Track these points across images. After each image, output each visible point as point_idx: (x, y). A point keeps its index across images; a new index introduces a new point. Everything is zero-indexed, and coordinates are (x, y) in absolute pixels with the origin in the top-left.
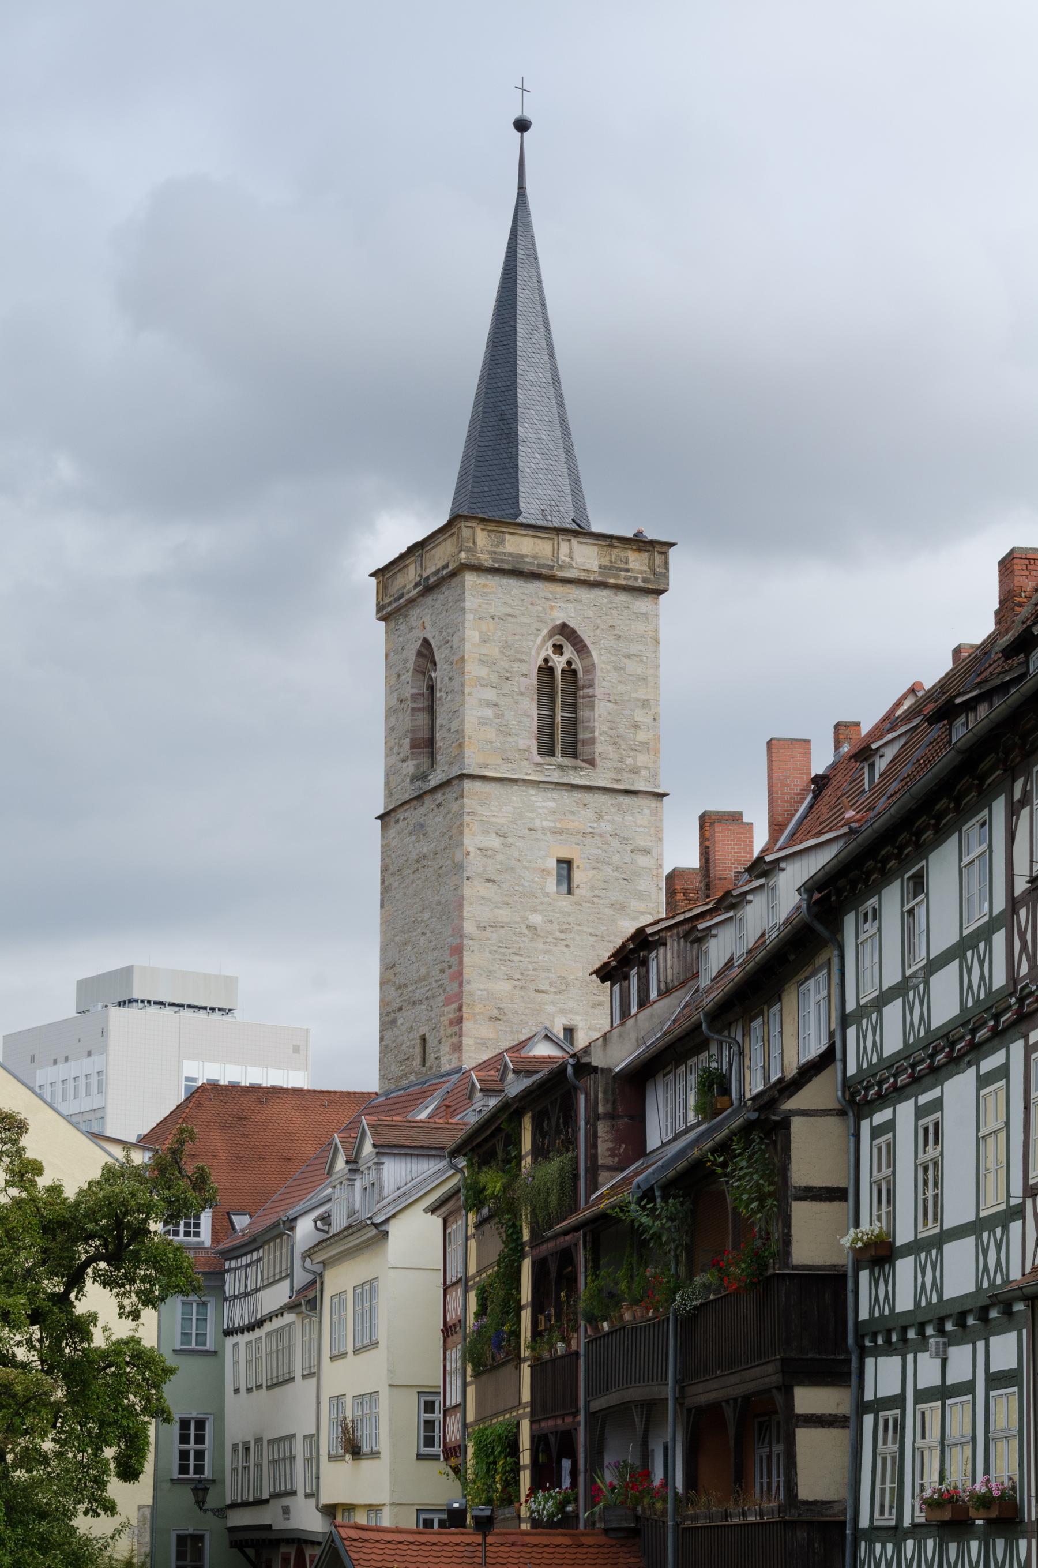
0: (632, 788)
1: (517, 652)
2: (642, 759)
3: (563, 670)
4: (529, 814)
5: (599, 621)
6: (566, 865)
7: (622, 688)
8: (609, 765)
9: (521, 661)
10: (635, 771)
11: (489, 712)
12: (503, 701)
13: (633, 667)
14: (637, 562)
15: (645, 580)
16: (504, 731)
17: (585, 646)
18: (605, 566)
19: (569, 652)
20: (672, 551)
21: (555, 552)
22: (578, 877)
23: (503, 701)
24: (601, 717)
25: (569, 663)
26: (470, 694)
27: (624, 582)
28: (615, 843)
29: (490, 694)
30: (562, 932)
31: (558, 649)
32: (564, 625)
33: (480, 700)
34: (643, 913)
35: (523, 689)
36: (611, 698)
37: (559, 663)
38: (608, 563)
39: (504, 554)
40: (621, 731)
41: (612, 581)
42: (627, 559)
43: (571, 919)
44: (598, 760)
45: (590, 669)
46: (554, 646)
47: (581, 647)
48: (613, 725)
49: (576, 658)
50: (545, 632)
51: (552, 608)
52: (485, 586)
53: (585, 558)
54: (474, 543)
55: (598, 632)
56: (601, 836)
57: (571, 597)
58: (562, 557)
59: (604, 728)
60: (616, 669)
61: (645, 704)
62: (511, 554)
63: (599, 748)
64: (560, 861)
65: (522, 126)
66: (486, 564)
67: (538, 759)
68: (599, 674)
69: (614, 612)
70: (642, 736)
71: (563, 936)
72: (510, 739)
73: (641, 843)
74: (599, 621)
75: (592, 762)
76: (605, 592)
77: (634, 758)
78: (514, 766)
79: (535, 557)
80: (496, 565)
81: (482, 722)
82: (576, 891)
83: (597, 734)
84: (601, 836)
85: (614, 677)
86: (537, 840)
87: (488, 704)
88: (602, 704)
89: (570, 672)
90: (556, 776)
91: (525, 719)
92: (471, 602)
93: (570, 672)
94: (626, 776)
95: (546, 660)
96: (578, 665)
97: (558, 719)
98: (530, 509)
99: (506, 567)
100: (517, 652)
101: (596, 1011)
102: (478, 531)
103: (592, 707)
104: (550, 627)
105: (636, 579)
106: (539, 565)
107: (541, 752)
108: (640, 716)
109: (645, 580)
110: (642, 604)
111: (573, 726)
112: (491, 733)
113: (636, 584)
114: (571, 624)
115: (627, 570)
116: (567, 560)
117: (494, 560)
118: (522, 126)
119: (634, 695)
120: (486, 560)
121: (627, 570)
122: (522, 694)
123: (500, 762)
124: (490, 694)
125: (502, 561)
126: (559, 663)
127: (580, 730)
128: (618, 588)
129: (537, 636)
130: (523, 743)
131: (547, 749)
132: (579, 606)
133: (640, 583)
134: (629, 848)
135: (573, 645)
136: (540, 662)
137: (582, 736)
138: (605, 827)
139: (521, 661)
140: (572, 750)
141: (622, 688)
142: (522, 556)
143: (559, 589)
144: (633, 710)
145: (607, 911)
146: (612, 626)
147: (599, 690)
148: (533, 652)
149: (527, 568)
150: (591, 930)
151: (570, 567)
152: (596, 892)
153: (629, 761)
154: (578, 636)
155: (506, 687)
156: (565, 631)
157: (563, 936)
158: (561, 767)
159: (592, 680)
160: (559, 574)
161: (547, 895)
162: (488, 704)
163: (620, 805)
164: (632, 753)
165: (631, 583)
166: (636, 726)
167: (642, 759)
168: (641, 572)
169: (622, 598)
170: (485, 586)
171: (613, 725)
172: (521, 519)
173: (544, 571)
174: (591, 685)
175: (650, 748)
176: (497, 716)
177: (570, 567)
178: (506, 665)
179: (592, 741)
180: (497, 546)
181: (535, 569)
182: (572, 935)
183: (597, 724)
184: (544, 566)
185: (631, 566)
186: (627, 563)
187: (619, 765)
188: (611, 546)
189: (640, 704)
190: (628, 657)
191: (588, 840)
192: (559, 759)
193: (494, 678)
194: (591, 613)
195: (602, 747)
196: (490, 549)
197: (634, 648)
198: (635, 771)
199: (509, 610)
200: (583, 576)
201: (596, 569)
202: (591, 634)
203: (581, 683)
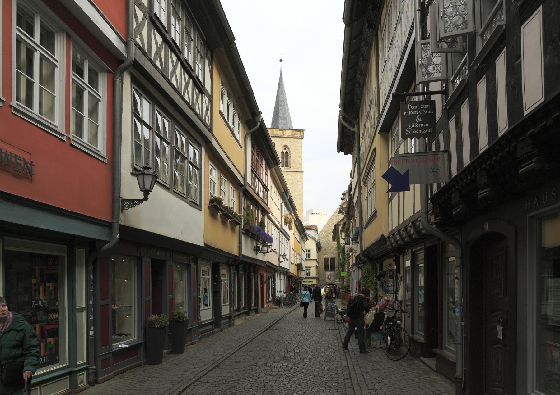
2: (299, 166)
10: (298, 168)
13: (297, 151)
14: (298, 134)
20: (304, 132)
24: (292, 160)
31: (285, 149)
37: (285, 151)
45: (290, 152)
53: (288, 133)
61: (300, 157)
65: (281, 61)
70: (299, 162)
89: (287, 153)
93: (287, 153)
108: (299, 159)
110: (299, 140)
111: (287, 162)
118: (281, 61)
126: (285, 151)
128: (295, 138)
138: (292, 178)
140: (287, 166)
147: (291, 155)
156: (285, 146)
167: (299, 166)
175: (301, 164)
198: (298, 168)
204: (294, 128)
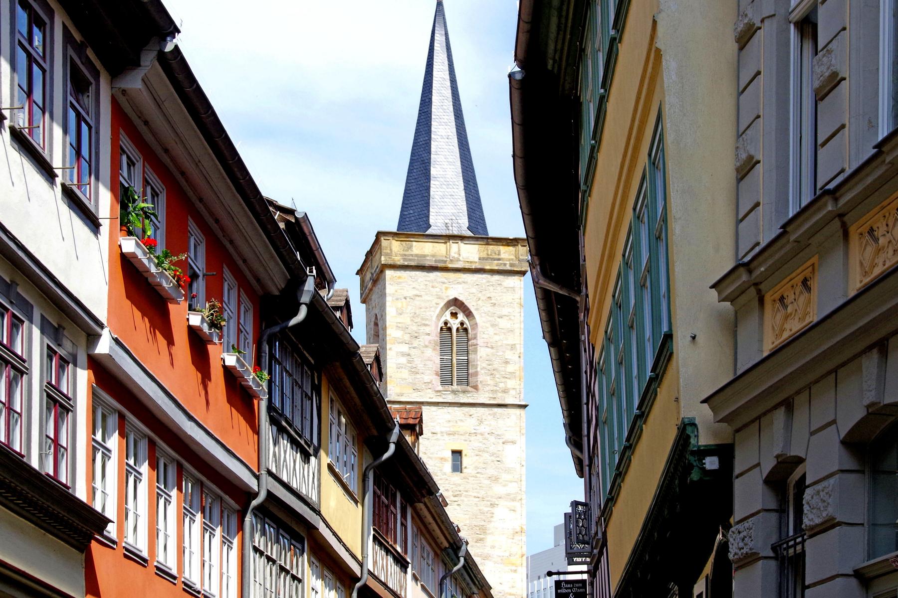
0: (503, 403)
1: (423, 319)
3: (458, 329)
4: (432, 424)
5: (480, 295)
6: (457, 453)
7: (497, 338)
8: (487, 388)
9: (426, 325)
10: (505, 391)
11: (403, 360)
12: (413, 352)
13: (503, 323)
15: (511, 265)
16: (414, 372)
17: (471, 312)
18: (484, 259)
19: (461, 317)
21: (448, 251)
22: (466, 461)
23: (413, 352)
25: (462, 324)
26: (390, 349)
27: (496, 268)
28: (492, 439)
29: (405, 348)
30: (455, 496)
31: (454, 315)
32: (456, 300)
33: (397, 353)
34: (511, 482)
35: (427, 343)
36: (489, 345)
37: (455, 324)
38: (485, 256)
39: (412, 255)
40: (496, 366)
41: (488, 267)
42: (499, 252)
43: (460, 488)
44: (480, 386)
46: (452, 313)
47: (468, 314)
48: (490, 361)
49: (466, 321)
50: (442, 304)
51: (447, 288)
52: (399, 277)
54: (391, 250)
55: (480, 302)
56: (482, 434)
57: (460, 280)
58: (453, 254)
59: (484, 365)
60: (493, 325)
62: (416, 255)
63: (480, 378)
64: (454, 452)
66: (399, 263)
67: (440, 388)
68: (480, 329)
69: (491, 288)
71: (456, 499)
72: (418, 376)
73: (508, 436)
74: (480, 295)
75: (476, 388)
76: (484, 276)
77: (505, 383)
78: (421, 393)
79: (433, 256)
80: (406, 263)
81: (399, 367)
82: (464, 470)
83: (479, 369)
84: (482, 434)
85: (491, 331)
86: (437, 439)
87: (403, 354)
88: (482, 349)
90: (450, 398)
91: (428, 363)
92: (390, 289)
94: (500, 395)
95: (446, 323)
96: (467, 324)
97: (455, 361)
98: (437, 224)
99: (412, 264)
100: (423, 319)
101: (478, 544)
102: (394, 242)
103: (475, 351)
104: (445, 301)
105: (505, 265)
106: (436, 261)
107: (443, 382)
109: (511, 265)
112: (405, 374)
113: (505, 268)
114: (460, 299)
115: (499, 259)
116: (456, 256)
117: (405, 260)
119: (505, 342)
120: (399, 261)
121: (499, 259)
122: (426, 346)
123: (412, 391)
124: (405, 348)
125: (410, 260)
126: (455, 324)
127: (470, 367)
129: (436, 308)
130: (427, 378)
131: (446, 380)
132: (466, 286)
133: (508, 268)
134: (501, 441)
135: (464, 312)
136: (441, 324)
137: (470, 371)
139: (426, 325)
141: (497, 338)
142: (425, 256)
143: (451, 275)
144: (504, 352)
145: (488, 482)
146: (489, 298)
147: (480, 341)
148: (434, 318)
149: (427, 263)
150: (476, 495)
151: (458, 260)
152: (479, 470)
153: (501, 385)
154: (466, 306)
155: (416, 343)
156: (457, 303)
157: (456, 499)
158: (454, 392)
159: (476, 334)
160: (450, 266)
161: (445, 474)
162: (403, 354)
163: (495, 414)
164: (504, 380)
165: (501, 268)
166: (507, 362)
168: (509, 260)
169: (497, 277)
170: (399, 277)
171: (490, 361)
172: (429, 232)
173: (440, 265)
174: (475, 338)
176: (409, 362)
177: (458, 260)
178: (415, 328)
179: (476, 374)
180: (407, 251)
181: (433, 264)
182: (462, 498)
183: (479, 363)
184: (440, 261)
185: (502, 256)
186: (499, 254)
187: (495, 388)
188: (488, 244)
189: (509, 347)
190: (500, 317)
191: (473, 438)
192: (455, 387)
193: (407, 337)
194: (474, 290)
195: (483, 377)
196: (402, 253)
197: (505, 311)
198: (505, 391)
199: (418, 293)
200: (467, 266)
201: (477, 260)
202: (475, 304)
203: (470, 336)
204: (491, 234)
